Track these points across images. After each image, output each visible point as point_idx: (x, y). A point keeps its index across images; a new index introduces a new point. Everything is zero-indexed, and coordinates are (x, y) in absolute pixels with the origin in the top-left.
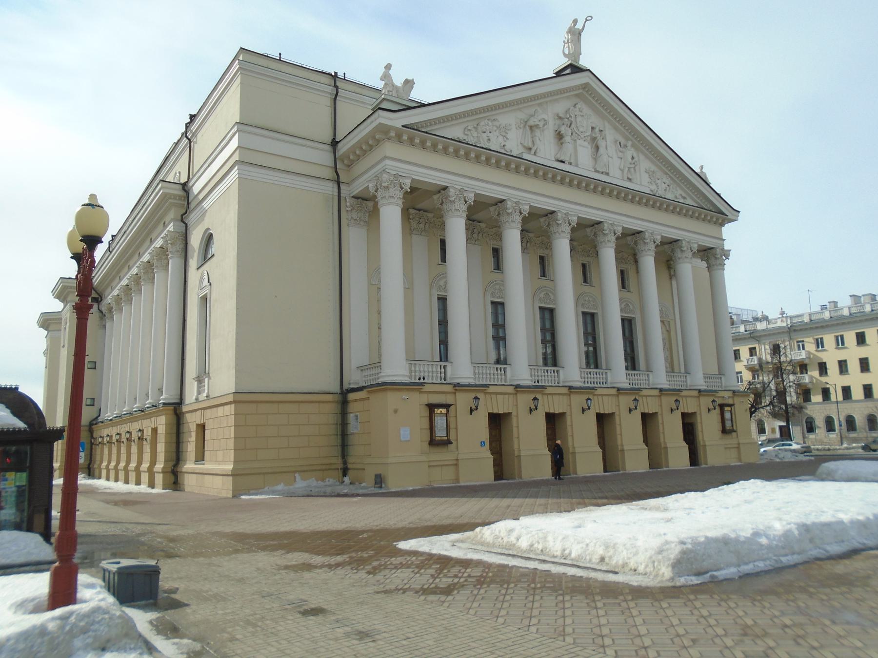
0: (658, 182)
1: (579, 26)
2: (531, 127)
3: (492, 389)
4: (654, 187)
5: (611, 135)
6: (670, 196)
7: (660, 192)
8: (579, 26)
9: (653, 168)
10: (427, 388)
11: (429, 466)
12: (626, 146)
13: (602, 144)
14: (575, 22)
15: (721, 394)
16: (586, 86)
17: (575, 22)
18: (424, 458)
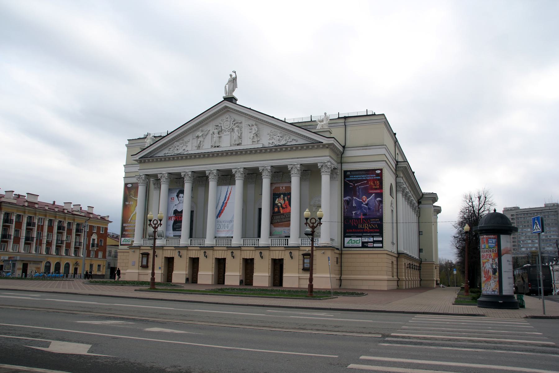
0: (275, 137)
1: (234, 76)
2: (198, 137)
3: (165, 248)
4: (271, 142)
5: (245, 122)
6: (283, 142)
7: (277, 143)
8: (234, 76)
9: (273, 130)
10: (142, 248)
11: (139, 274)
12: (253, 125)
13: (236, 129)
14: (231, 75)
15: (301, 248)
16: (226, 107)
17: (231, 75)
18: (137, 271)
